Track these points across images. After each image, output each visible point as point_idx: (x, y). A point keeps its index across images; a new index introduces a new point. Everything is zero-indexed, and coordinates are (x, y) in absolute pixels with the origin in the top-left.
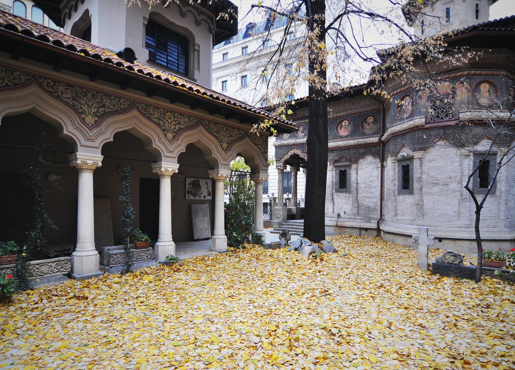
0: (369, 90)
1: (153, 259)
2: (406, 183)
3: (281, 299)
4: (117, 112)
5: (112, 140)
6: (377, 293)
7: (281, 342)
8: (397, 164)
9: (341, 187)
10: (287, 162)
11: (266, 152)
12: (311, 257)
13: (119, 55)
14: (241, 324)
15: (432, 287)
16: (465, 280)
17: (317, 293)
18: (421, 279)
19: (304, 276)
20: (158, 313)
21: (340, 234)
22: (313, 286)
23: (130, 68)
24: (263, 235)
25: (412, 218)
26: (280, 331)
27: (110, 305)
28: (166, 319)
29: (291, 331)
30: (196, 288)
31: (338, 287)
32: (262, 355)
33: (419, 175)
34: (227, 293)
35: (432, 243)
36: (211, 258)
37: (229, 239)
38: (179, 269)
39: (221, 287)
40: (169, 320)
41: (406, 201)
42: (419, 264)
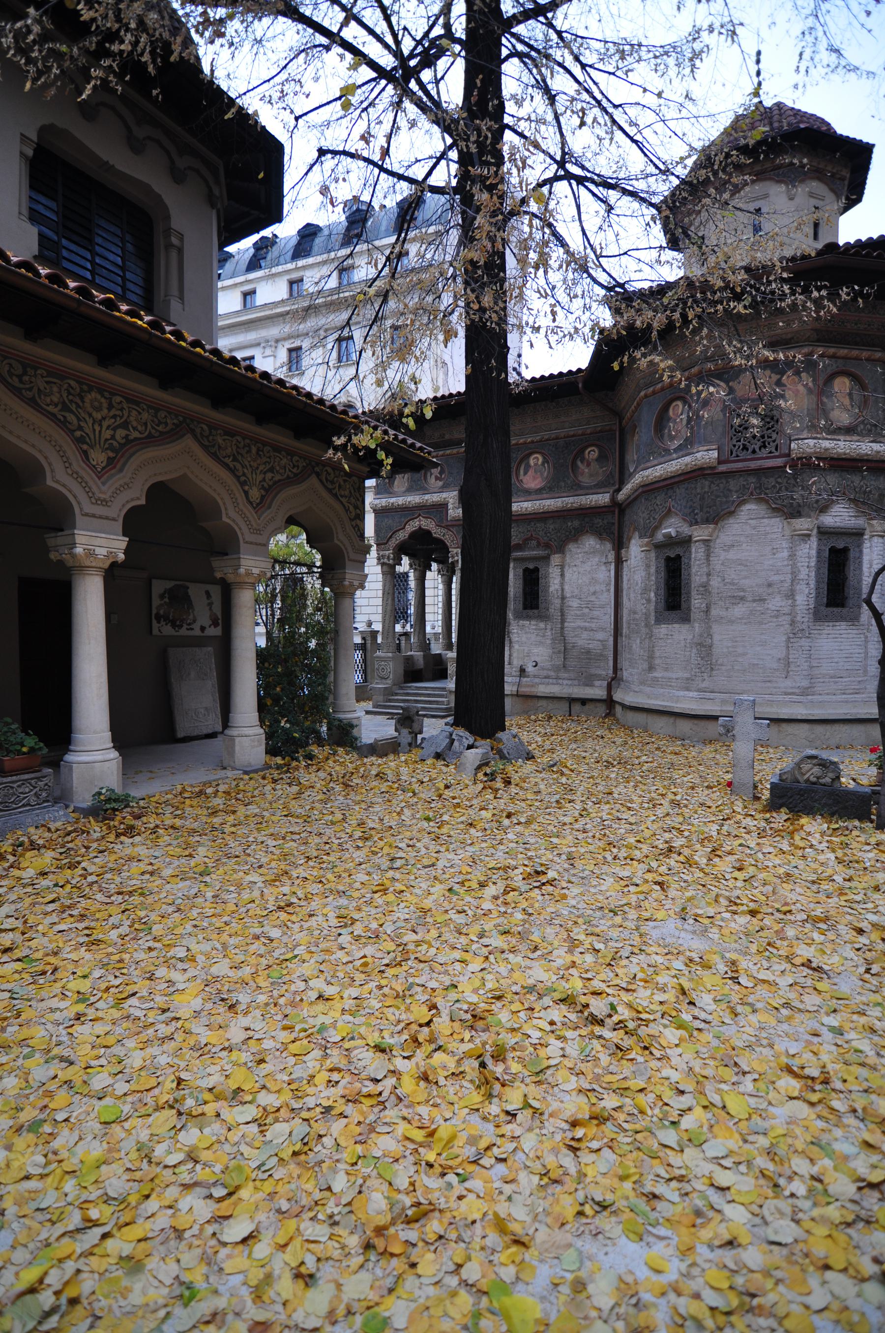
0: (626, 359)
1: (57, 801)
2: (674, 597)
3: (428, 903)
6: (663, 869)
7: (452, 1064)
8: (653, 555)
9: (525, 608)
10: (402, 549)
14: (321, 1007)
17: (517, 877)
20: (57, 988)
21: (526, 712)
22: (500, 857)
24: (355, 722)
25: (687, 675)
26: (442, 1024)
28: (81, 1008)
29: (476, 1019)
30: (181, 885)
31: (564, 857)
32: (402, 1128)
33: (704, 579)
34: (272, 895)
36: (222, 788)
37: (269, 736)
38: (132, 828)
39: (254, 877)
41: (675, 637)
42: (735, 784)
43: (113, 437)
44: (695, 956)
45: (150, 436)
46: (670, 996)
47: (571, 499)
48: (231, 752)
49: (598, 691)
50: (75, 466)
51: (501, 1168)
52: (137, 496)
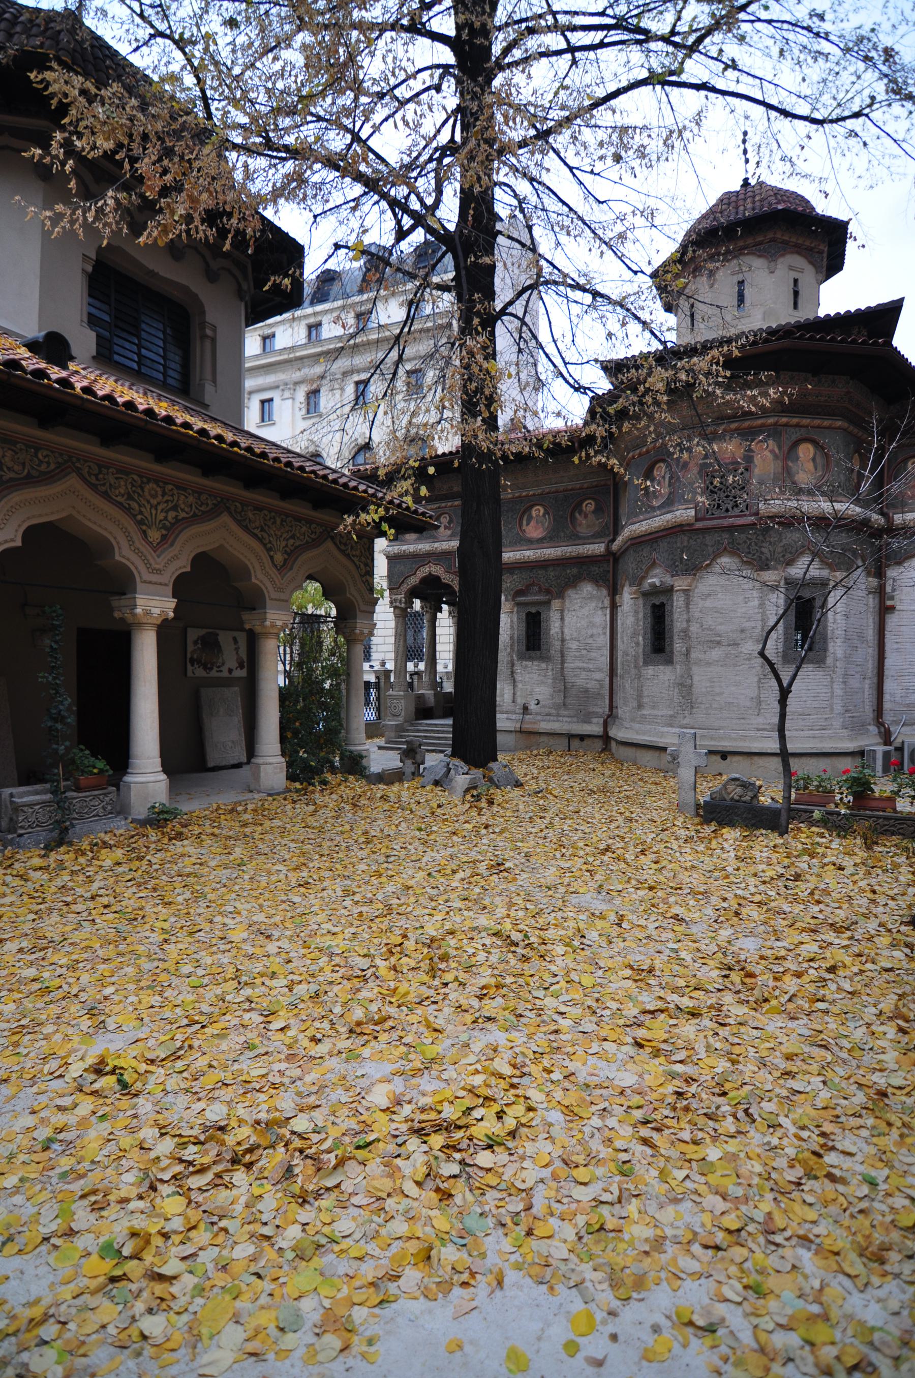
1: (118, 813)
2: (659, 642)
3: (411, 883)
4: (29, 481)
5: (18, 543)
8: (641, 601)
9: (528, 649)
10: (414, 593)
11: (370, 573)
12: (468, 797)
13: (33, 346)
14: (329, 937)
15: (701, 848)
16: (757, 833)
17: (482, 868)
18: (683, 833)
19: (455, 838)
20: (147, 926)
21: (529, 748)
22: (473, 855)
23: (65, 383)
25: (670, 713)
26: (410, 945)
27: (33, 916)
32: (376, 990)
34: (293, 878)
35: (703, 761)
36: (250, 807)
37: (289, 765)
38: (181, 833)
39: (279, 867)
40: (173, 939)
41: (660, 679)
43: (166, 518)
44: (597, 913)
45: (195, 515)
46: (570, 933)
47: (570, 549)
48: (257, 776)
49: (595, 728)
50: (137, 544)
51: (434, 1006)
52: (183, 565)
